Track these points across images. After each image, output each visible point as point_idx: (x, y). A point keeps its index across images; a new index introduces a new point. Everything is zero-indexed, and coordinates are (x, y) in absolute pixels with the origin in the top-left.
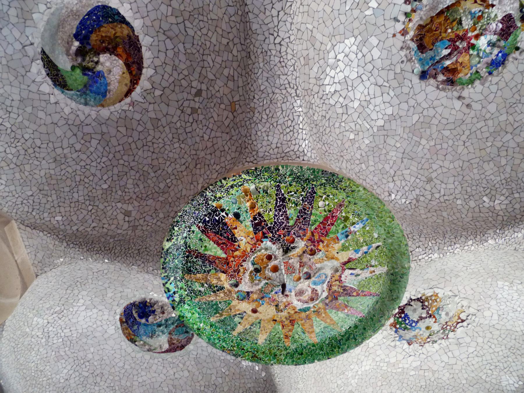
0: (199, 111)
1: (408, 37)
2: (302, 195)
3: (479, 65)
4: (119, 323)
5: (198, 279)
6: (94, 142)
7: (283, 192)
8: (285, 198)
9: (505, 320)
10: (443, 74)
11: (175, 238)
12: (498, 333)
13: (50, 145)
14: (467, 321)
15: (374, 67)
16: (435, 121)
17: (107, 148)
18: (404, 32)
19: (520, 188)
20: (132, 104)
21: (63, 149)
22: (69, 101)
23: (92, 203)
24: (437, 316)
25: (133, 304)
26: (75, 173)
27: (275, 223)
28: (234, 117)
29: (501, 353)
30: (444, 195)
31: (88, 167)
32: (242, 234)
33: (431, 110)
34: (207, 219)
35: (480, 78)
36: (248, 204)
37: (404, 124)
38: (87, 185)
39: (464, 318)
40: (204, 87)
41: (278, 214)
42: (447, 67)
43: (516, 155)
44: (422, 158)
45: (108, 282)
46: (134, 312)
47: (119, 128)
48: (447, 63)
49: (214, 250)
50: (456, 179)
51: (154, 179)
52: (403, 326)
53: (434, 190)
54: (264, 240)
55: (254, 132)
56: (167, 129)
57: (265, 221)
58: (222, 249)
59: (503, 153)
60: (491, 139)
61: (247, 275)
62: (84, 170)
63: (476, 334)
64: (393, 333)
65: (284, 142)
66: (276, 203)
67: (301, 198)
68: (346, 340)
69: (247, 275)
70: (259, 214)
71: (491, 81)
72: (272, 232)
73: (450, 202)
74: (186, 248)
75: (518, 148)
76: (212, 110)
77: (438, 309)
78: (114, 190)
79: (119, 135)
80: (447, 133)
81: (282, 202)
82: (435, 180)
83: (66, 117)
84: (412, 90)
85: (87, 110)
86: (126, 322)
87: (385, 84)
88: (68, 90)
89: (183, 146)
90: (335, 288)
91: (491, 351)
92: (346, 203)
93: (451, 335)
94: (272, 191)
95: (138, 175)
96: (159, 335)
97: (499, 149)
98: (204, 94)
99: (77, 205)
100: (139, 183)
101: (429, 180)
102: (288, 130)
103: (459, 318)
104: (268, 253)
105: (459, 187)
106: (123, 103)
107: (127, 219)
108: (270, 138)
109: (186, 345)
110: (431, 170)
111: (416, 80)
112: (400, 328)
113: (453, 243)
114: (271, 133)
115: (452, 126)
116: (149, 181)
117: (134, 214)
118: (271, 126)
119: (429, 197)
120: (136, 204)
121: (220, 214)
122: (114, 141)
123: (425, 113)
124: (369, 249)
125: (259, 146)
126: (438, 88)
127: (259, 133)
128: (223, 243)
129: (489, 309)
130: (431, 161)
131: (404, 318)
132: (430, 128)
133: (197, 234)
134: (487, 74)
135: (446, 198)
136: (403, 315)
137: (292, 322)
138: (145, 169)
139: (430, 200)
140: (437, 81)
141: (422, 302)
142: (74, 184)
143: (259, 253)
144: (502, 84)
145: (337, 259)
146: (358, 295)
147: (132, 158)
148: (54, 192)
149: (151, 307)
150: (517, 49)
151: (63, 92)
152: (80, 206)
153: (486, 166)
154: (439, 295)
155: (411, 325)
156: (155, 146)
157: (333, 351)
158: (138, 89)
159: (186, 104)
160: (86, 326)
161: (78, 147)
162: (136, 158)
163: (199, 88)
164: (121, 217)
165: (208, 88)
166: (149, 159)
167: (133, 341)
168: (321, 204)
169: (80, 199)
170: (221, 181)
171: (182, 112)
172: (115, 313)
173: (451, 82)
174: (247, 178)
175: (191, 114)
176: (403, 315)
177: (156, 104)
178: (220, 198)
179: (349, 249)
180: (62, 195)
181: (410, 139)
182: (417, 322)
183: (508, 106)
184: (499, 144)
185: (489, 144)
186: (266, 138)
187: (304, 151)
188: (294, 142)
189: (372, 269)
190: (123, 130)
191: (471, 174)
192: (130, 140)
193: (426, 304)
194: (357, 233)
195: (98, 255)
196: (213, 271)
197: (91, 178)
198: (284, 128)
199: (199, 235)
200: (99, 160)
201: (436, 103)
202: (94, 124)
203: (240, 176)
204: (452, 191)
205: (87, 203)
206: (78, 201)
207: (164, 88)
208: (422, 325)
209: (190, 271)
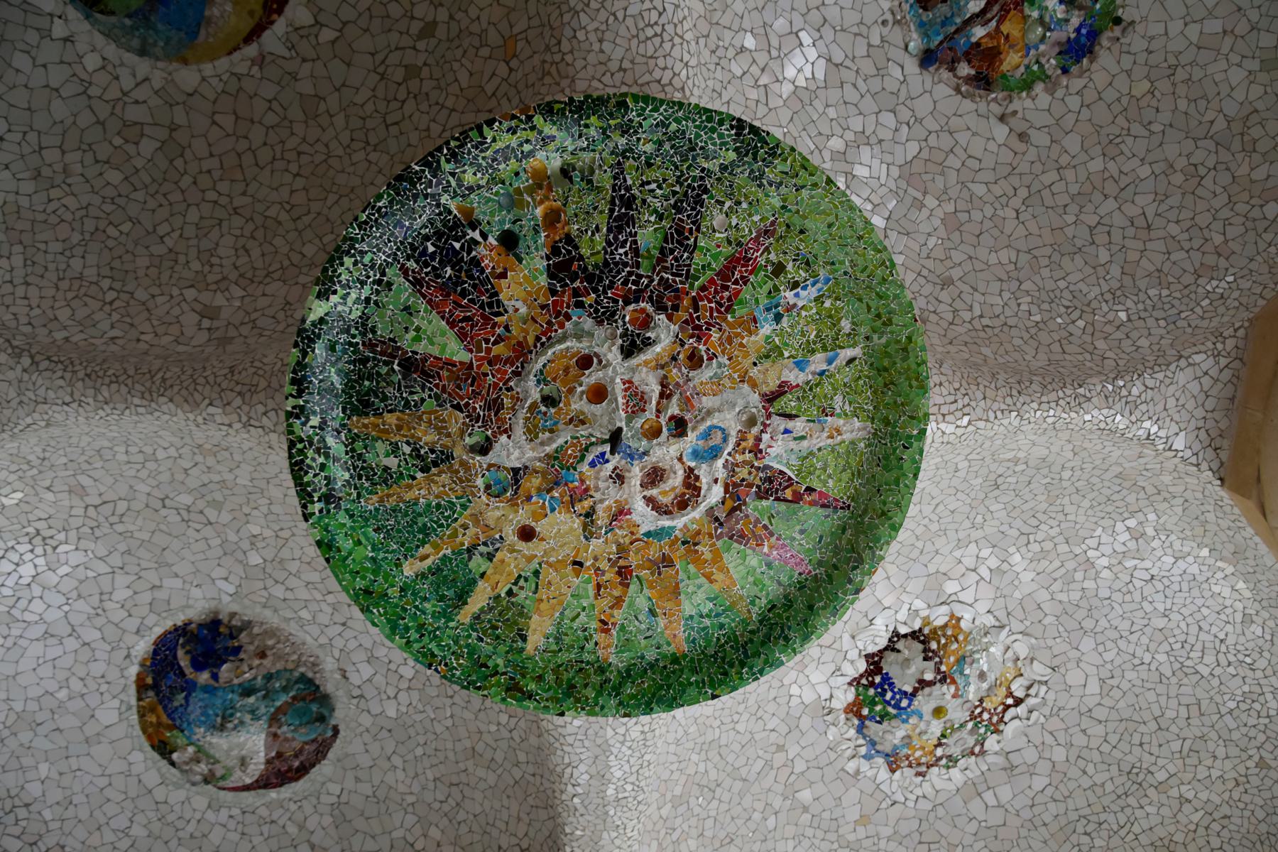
0: (425, 72)
2: (674, 193)
3: (1042, 47)
4: (132, 690)
5: (387, 432)
6: (148, 147)
7: (630, 182)
8: (634, 197)
9: (1116, 694)
10: (969, 62)
11: (341, 292)
12: (1099, 730)
13: (32, 137)
14: (1031, 701)
15: (825, 20)
16: (954, 162)
17: (179, 163)
19: (1145, 310)
20: (260, 61)
21: (63, 152)
22: (99, 40)
23: (117, 285)
24: (957, 677)
25: (181, 631)
26: (83, 212)
27: (606, 263)
28: (511, 70)
29: (1109, 787)
30: (981, 316)
31: (121, 201)
32: (517, 291)
33: (945, 136)
34: (431, 249)
35: (1044, 77)
36: (539, 212)
37: (889, 158)
38: (111, 243)
39: (1019, 693)
40: (442, 15)
41: (616, 238)
42: (978, 44)
43: (1128, 243)
44: (929, 235)
45: (122, 547)
46: (180, 653)
47: (217, 117)
48: (979, 32)
49: (438, 339)
50: (1005, 286)
51: (292, 236)
52: (878, 708)
53: (958, 304)
54: (575, 313)
55: (568, 32)
56: (339, 120)
57: (581, 258)
58: (462, 336)
59: (1101, 238)
60: (1073, 208)
61: (523, 413)
62: (108, 208)
63: (1049, 740)
64: (852, 732)
65: (639, 59)
66: (612, 211)
67: (672, 202)
68: (763, 643)
69: (523, 413)
70: (569, 239)
71: (1067, 87)
72: (595, 290)
73: (996, 331)
74: (364, 334)
75: (1133, 229)
76: (456, 66)
77: (961, 660)
78: (182, 259)
79: (215, 133)
80: (980, 190)
81: (624, 211)
82: (958, 283)
83: (85, 76)
84: (904, 85)
85: (143, 66)
86: (155, 687)
87: (848, 63)
88: (102, 12)
89: (374, 156)
90: (743, 473)
91: (1086, 782)
92: (781, 230)
93: (991, 743)
94: (604, 179)
95: (251, 226)
96: (242, 723)
97: (1091, 229)
98: (441, 32)
99: (76, 287)
100: (251, 244)
101: (947, 283)
102: (650, 32)
103: (1010, 694)
104: (582, 346)
105: (1013, 304)
106: (237, 56)
107: (206, 323)
108: (606, 46)
109: (313, 765)
110: (948, 263)
111: (912, 66)
112: (872, 718)
113: (1014, 392)
114: (608, 36)
115: (989, 176)
116: (278, 241)
117: (225, 314)
118: (612, 18)
119: (949, 317)
120: (237, 292)
121: (465, 234)
122: (199, 146)
123: (933, 140)
124: (830, 362)
125: (579, 64)
126: (957, 90)
127: (581, 35)
128: (466, 319)
129: (1079, 661)
130: (948, 244)
131: (881, 685)
132: (942, 174)
133: (399, 292)
134: (1059, 72)
135: (985, 321)
136: (878, 679)
138: (272, 212)
139: (951, 324)
140: (955, 76)
141: (923, 642)
142: (76, 238)
143: (559, 347)
144: (1090, 96)
146: (797, 498)
147: (240, 187)
148: (18, 249)
149: (232, 637)
150: (1117, 21)
151: (87, 17)
152: (83, 291)
153: (1066, 261)
154: (963, 624)
155: (897, 706)
156: (305, 159)
157: (725, 674)
158: (280, 26)
159: (394, 58)
160: (34, 692)
161: (103, 151)
162: (251, 190)
163: (430, 18)
164: (191, 319)
165: (451, 17)
166: (285, 192)
167: (164, 749)
168: (718, 219)
169: (86, 272)
170: (479, 128)
171: (382, 78)
172: (128, 656)
173: (983, 82)
174: (549, 130)
175: (405, 80)
176: (878, 679)
177: (319, 64)
178: (471, 189)
179: (781, 354)
180: (39, 258)
181: (901, 193)
182: (914, 694)
183: (1105, 141)
184: (1093, 220)
185: (1070, 219)
186: (596, 47)
187: (683, 89)
188: (661, 62)
190: (227, 121)
191: (1037, 279)
192: (242, 145)
193: (934, 645)
194: (804, 313)
195: (114, 386)
196: (430, 404)
197: (126, 227)
198: (641, 25)
199: (404, 297)
200: (152, 190)
201: (955, 122)
202: (155, 101)
203: (530, 118)
204: (998, 310)
205: (106, 284)
206: (81, 278)
207: (345, 24)
208: (925, 703)
209: (367, 404)
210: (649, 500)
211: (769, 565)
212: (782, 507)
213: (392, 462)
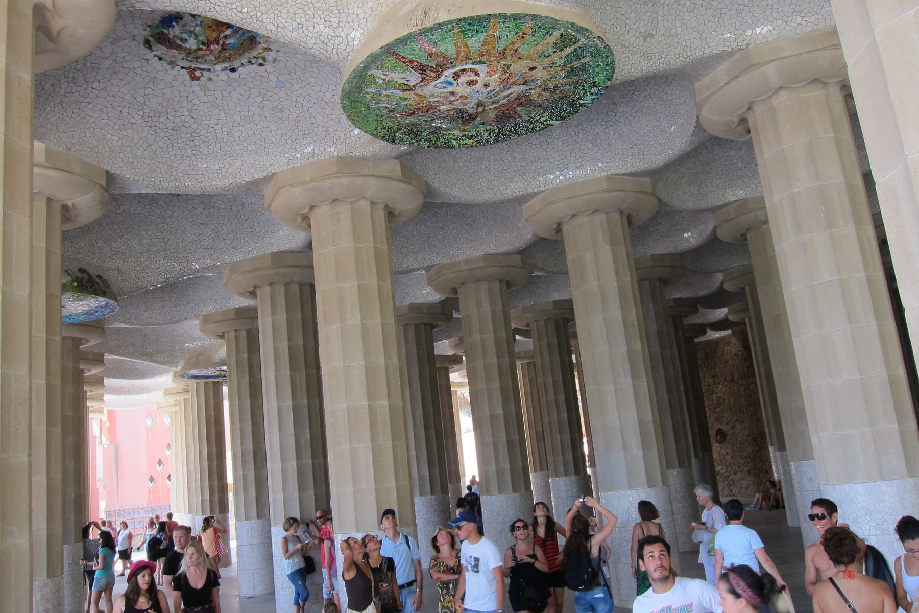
1: (264, 45)
18: (267, 49)
90: (432, 74)
137: (503, 54)
145: (416, 94)
146: (411, 62)
174: (454, 143)
189: (383, 77)
210: (477, 74)
211: (435, 43)
212: (420, 61)
213: (567, 87)
